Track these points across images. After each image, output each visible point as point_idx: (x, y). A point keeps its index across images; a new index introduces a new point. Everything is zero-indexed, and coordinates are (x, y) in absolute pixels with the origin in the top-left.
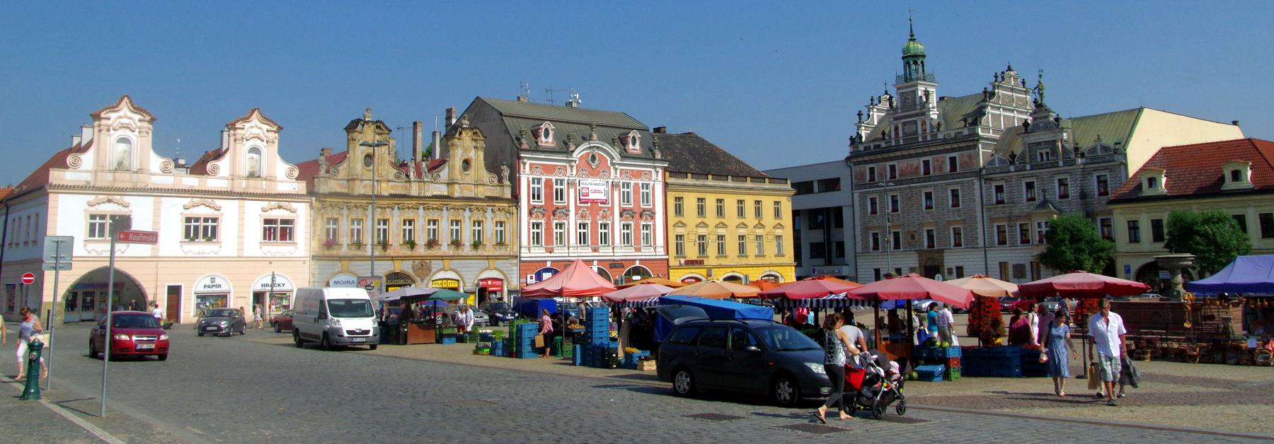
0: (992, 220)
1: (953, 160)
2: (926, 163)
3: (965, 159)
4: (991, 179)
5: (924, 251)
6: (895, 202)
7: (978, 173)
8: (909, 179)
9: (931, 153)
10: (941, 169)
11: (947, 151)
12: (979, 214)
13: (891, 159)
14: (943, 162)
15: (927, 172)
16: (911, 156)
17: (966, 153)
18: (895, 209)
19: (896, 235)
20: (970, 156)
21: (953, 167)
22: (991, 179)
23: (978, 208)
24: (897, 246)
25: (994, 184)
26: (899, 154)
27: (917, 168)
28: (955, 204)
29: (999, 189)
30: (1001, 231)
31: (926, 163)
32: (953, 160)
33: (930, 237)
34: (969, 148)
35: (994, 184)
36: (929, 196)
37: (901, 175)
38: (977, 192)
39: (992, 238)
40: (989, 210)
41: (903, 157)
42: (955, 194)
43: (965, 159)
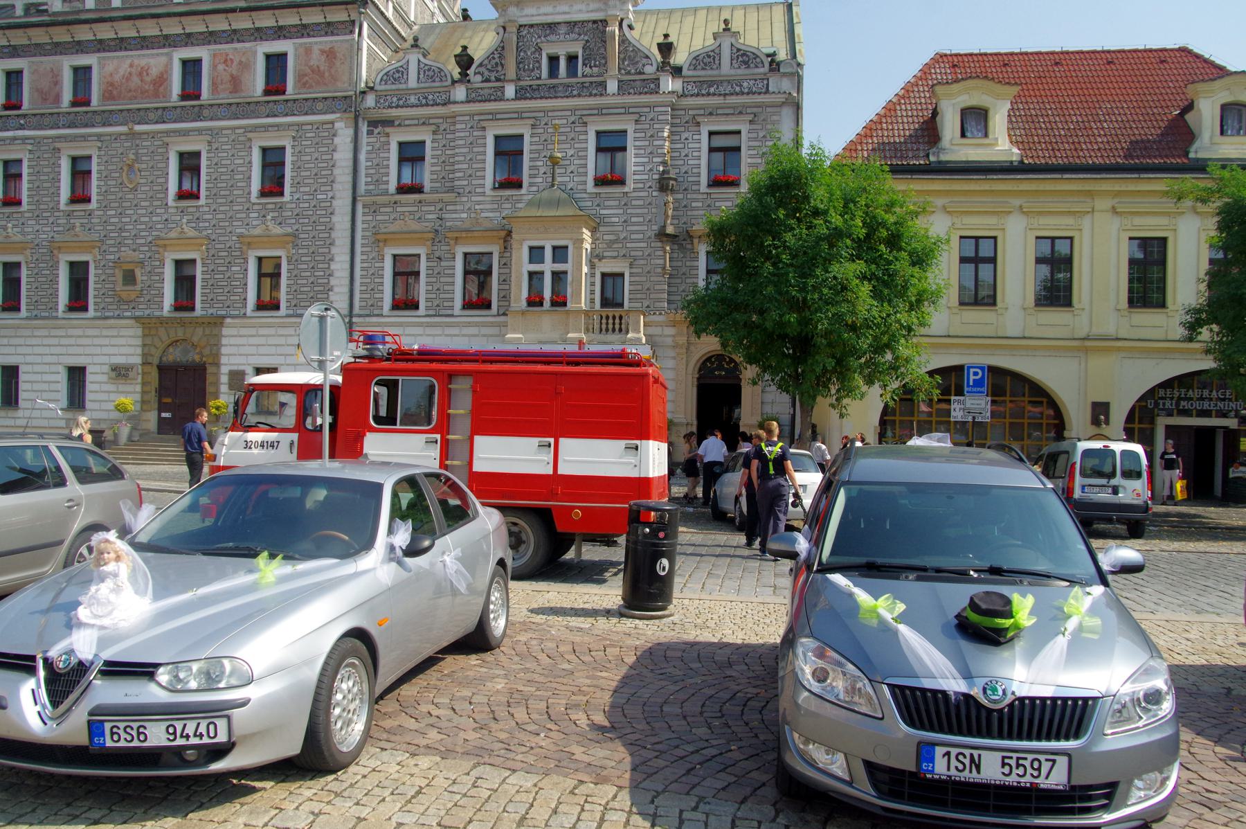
0: (379, 240)
1: (276, 63)
2: (191, 68)
3: (316, 59)
4: (389, 123)
5: (162, 321)
6: (80, 173)
7: (350, 105)
8: (136, 107)
9: (211, 37)
10: (236, 84)
11: (260, 34)
12: (341, 221)
13: (80, 47)
14: (246, 66)
15: (191, 92)
16: (144, 43)
17: (320, 42)
18: (79, 197)
19: (79, 274)
20: (330, 54)
21: (275, 86)
22: (389, 123)
23: (342, 204)
24: (78, 302)
25: (397, 137)
26: (105, 32)
27: (162, 80)
28: (273, 187)
29: (411, 154)
30: (405, 272)
31: (191, 68)
32: (276, 63)
33: (185, 283)
34: (329, 28)
35: (397, 137)
36: (190, 164)
37: (108, 96)
38: (343, 156)
39: (374, 289)
40: (373, 209)
41: (121, 44)
42: (273, 161)
43: (316, 59)
